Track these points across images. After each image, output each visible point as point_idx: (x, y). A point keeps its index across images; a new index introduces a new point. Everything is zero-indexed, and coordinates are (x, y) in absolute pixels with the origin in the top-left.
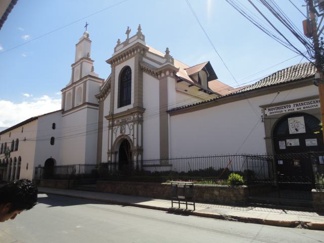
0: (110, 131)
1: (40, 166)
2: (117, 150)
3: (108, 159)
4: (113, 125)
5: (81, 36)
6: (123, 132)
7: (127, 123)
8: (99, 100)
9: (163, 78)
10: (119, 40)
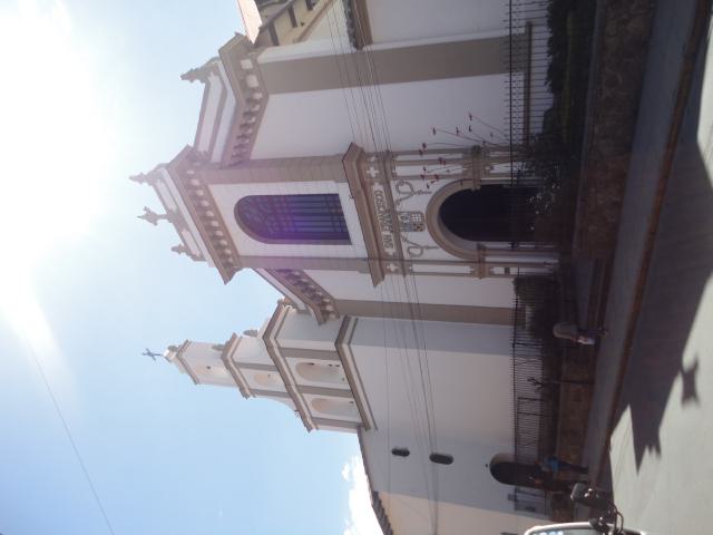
0: (416, 268)
1: (513, 498)
2: (473, 245)
3: (499, 276)
4: (399, 259)
5: (174, 368)
6: (417, 219)
7: (392, 204)
8: (333, 316)
9: (261, 80)
10: (173, 249)
